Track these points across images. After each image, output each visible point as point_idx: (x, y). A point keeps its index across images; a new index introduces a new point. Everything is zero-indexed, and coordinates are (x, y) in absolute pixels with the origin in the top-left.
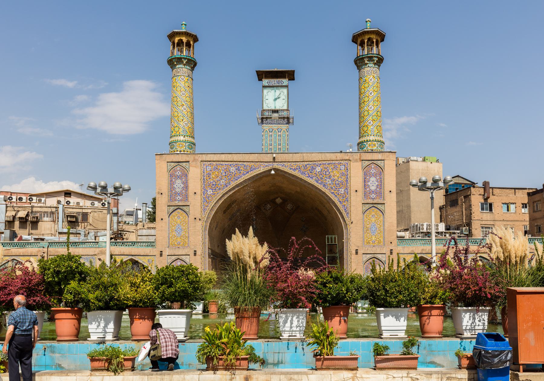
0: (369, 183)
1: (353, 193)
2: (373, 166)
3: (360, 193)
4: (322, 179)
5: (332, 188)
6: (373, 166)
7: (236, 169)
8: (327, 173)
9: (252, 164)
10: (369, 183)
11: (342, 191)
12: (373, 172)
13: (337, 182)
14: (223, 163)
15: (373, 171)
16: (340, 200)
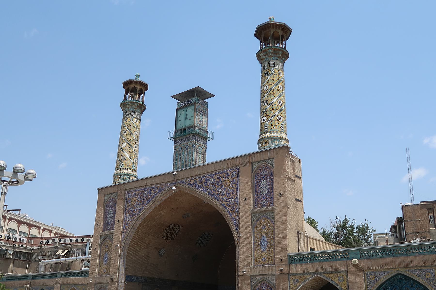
0: (260, 188)
1: (242, 202)
2: (264, 167)
3: (250, 201)
4: (214, 190)
5: (223, 199)
6: (264, 167)
7: (148, 193)
8: (220, 183)
9: (160, 185)
10: (260, 188)
11: (232, 201)
12: (263, 174)
13: (228, 192)
14: (139, 189)
15: (264, 173)
16: (231, 212)
